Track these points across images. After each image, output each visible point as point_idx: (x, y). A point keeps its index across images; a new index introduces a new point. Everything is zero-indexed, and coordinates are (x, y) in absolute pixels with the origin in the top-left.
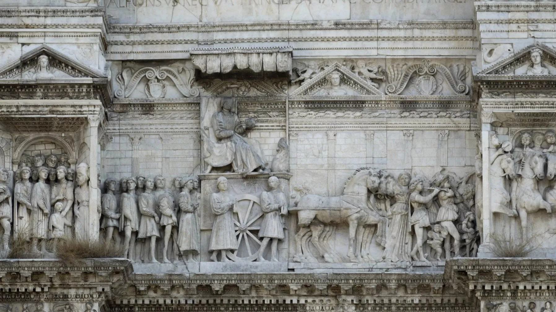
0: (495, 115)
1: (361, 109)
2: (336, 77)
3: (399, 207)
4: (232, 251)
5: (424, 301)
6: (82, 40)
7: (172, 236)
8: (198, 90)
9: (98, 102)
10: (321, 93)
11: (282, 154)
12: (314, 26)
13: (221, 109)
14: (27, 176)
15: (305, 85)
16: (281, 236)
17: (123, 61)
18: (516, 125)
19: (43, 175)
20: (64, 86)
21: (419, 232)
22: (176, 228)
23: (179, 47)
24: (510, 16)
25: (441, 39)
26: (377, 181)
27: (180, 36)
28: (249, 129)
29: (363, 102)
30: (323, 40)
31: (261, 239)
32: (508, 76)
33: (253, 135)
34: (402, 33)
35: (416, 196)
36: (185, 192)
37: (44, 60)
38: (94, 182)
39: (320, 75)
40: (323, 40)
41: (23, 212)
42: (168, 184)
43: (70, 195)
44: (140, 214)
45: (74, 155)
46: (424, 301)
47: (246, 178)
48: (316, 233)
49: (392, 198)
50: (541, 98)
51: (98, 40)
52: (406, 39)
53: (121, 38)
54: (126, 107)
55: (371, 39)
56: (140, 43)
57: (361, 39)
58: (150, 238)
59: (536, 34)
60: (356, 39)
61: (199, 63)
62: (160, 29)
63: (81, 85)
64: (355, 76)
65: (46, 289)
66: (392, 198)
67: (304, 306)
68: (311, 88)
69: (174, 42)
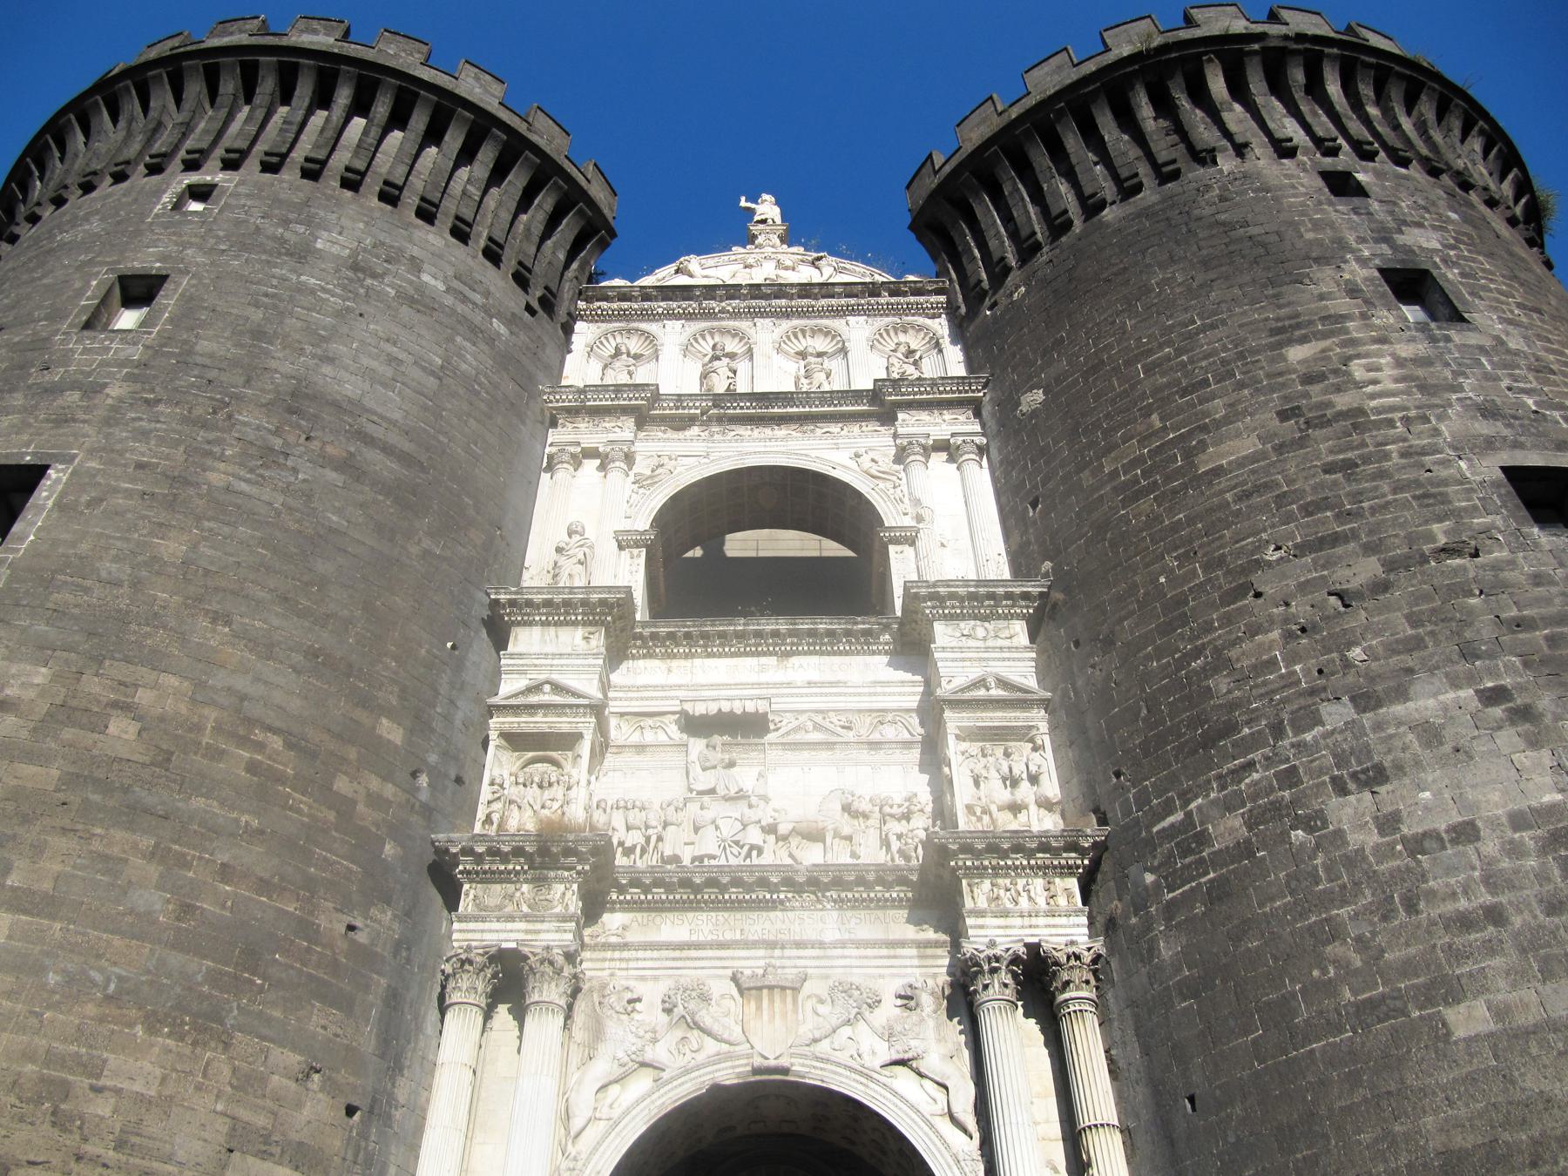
0: (959, 727)
1: (832, 749)
2: (810, 724)
3: (874, 821)
4: (714, 857)
5: (902, 895)
6: (583, 676)
7: (656, 847)
8: (685, 736)
9: (594, 720)
10: (799, 737)
11: (761, 780)
12: (789, 685)
13: (707, 746)
14: (521, 780)
15: (781, 732)
16: (761, 843)
17: (622, 715)
18: (979, 741)
19: (536, 779)
20: (564, 706)
21: (893, 839)
22: (660, 839)
23: (671, 702)
24: (963, 655)
25: (900, 694)
26: (850, 798)
27: (672, 693)
28: (731, 764)
29: (835, 743)
30: (797, 695)
31: (742, 847)
32: (967, 695)
33: (734, 770)
34: (866, 690)
35: (887, 809)
36: (672, 808)
37: (547, 688)
38: (583, 783)
39: (795, 723)
40: (797, 695)
41: (514, 808)
42: (656, 806)
43: (560, 796)
44: (628, 828)
45: (568, 767)
46: (902, 895)
47: (727, 799)
48: (795, 841)
49: (866, 816)
50: (999, 714)
51: (597, 676)
52: (870, 694)
53: (620, 695)
54: (621, 748)
55: (840, 694)
56: (637, 699)
57: (831, 694)
58: (634, 847)
59: (988, 669)
60: (826, 695)
61: (688, 707)
62: (655, 687)
63: (578, 706)
64: (826, 724)
65: (526, 867)
66: (866, 816)
67: (782, 902)
68: (788, 733)
69: (667, 698)
